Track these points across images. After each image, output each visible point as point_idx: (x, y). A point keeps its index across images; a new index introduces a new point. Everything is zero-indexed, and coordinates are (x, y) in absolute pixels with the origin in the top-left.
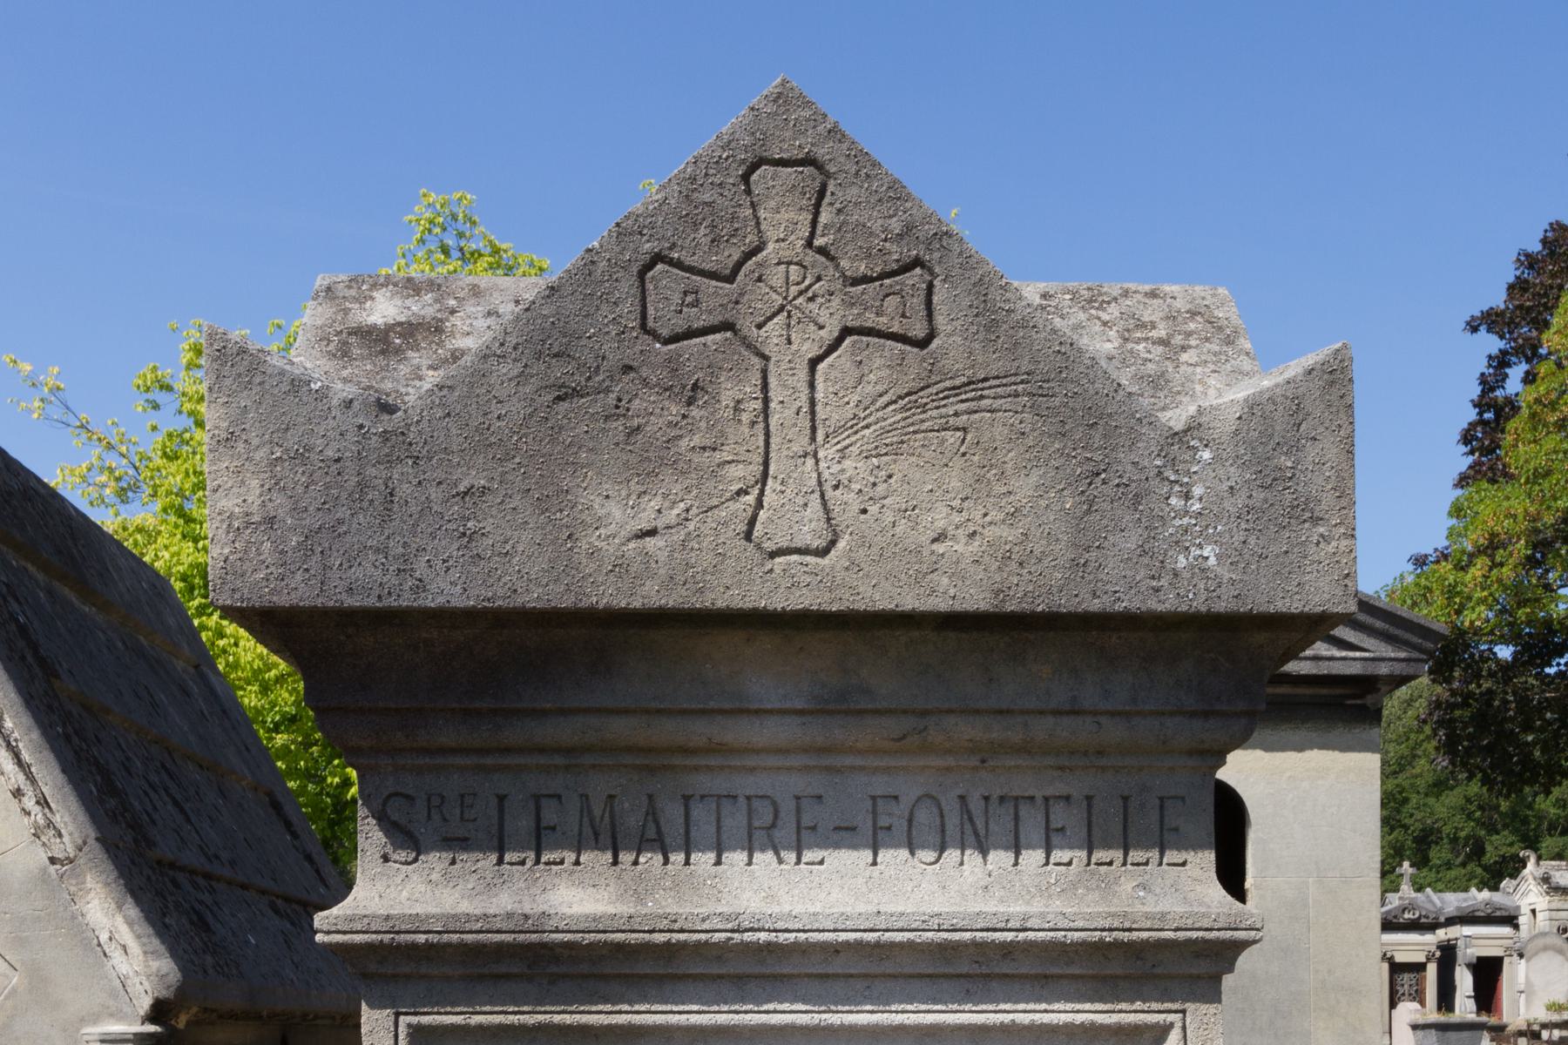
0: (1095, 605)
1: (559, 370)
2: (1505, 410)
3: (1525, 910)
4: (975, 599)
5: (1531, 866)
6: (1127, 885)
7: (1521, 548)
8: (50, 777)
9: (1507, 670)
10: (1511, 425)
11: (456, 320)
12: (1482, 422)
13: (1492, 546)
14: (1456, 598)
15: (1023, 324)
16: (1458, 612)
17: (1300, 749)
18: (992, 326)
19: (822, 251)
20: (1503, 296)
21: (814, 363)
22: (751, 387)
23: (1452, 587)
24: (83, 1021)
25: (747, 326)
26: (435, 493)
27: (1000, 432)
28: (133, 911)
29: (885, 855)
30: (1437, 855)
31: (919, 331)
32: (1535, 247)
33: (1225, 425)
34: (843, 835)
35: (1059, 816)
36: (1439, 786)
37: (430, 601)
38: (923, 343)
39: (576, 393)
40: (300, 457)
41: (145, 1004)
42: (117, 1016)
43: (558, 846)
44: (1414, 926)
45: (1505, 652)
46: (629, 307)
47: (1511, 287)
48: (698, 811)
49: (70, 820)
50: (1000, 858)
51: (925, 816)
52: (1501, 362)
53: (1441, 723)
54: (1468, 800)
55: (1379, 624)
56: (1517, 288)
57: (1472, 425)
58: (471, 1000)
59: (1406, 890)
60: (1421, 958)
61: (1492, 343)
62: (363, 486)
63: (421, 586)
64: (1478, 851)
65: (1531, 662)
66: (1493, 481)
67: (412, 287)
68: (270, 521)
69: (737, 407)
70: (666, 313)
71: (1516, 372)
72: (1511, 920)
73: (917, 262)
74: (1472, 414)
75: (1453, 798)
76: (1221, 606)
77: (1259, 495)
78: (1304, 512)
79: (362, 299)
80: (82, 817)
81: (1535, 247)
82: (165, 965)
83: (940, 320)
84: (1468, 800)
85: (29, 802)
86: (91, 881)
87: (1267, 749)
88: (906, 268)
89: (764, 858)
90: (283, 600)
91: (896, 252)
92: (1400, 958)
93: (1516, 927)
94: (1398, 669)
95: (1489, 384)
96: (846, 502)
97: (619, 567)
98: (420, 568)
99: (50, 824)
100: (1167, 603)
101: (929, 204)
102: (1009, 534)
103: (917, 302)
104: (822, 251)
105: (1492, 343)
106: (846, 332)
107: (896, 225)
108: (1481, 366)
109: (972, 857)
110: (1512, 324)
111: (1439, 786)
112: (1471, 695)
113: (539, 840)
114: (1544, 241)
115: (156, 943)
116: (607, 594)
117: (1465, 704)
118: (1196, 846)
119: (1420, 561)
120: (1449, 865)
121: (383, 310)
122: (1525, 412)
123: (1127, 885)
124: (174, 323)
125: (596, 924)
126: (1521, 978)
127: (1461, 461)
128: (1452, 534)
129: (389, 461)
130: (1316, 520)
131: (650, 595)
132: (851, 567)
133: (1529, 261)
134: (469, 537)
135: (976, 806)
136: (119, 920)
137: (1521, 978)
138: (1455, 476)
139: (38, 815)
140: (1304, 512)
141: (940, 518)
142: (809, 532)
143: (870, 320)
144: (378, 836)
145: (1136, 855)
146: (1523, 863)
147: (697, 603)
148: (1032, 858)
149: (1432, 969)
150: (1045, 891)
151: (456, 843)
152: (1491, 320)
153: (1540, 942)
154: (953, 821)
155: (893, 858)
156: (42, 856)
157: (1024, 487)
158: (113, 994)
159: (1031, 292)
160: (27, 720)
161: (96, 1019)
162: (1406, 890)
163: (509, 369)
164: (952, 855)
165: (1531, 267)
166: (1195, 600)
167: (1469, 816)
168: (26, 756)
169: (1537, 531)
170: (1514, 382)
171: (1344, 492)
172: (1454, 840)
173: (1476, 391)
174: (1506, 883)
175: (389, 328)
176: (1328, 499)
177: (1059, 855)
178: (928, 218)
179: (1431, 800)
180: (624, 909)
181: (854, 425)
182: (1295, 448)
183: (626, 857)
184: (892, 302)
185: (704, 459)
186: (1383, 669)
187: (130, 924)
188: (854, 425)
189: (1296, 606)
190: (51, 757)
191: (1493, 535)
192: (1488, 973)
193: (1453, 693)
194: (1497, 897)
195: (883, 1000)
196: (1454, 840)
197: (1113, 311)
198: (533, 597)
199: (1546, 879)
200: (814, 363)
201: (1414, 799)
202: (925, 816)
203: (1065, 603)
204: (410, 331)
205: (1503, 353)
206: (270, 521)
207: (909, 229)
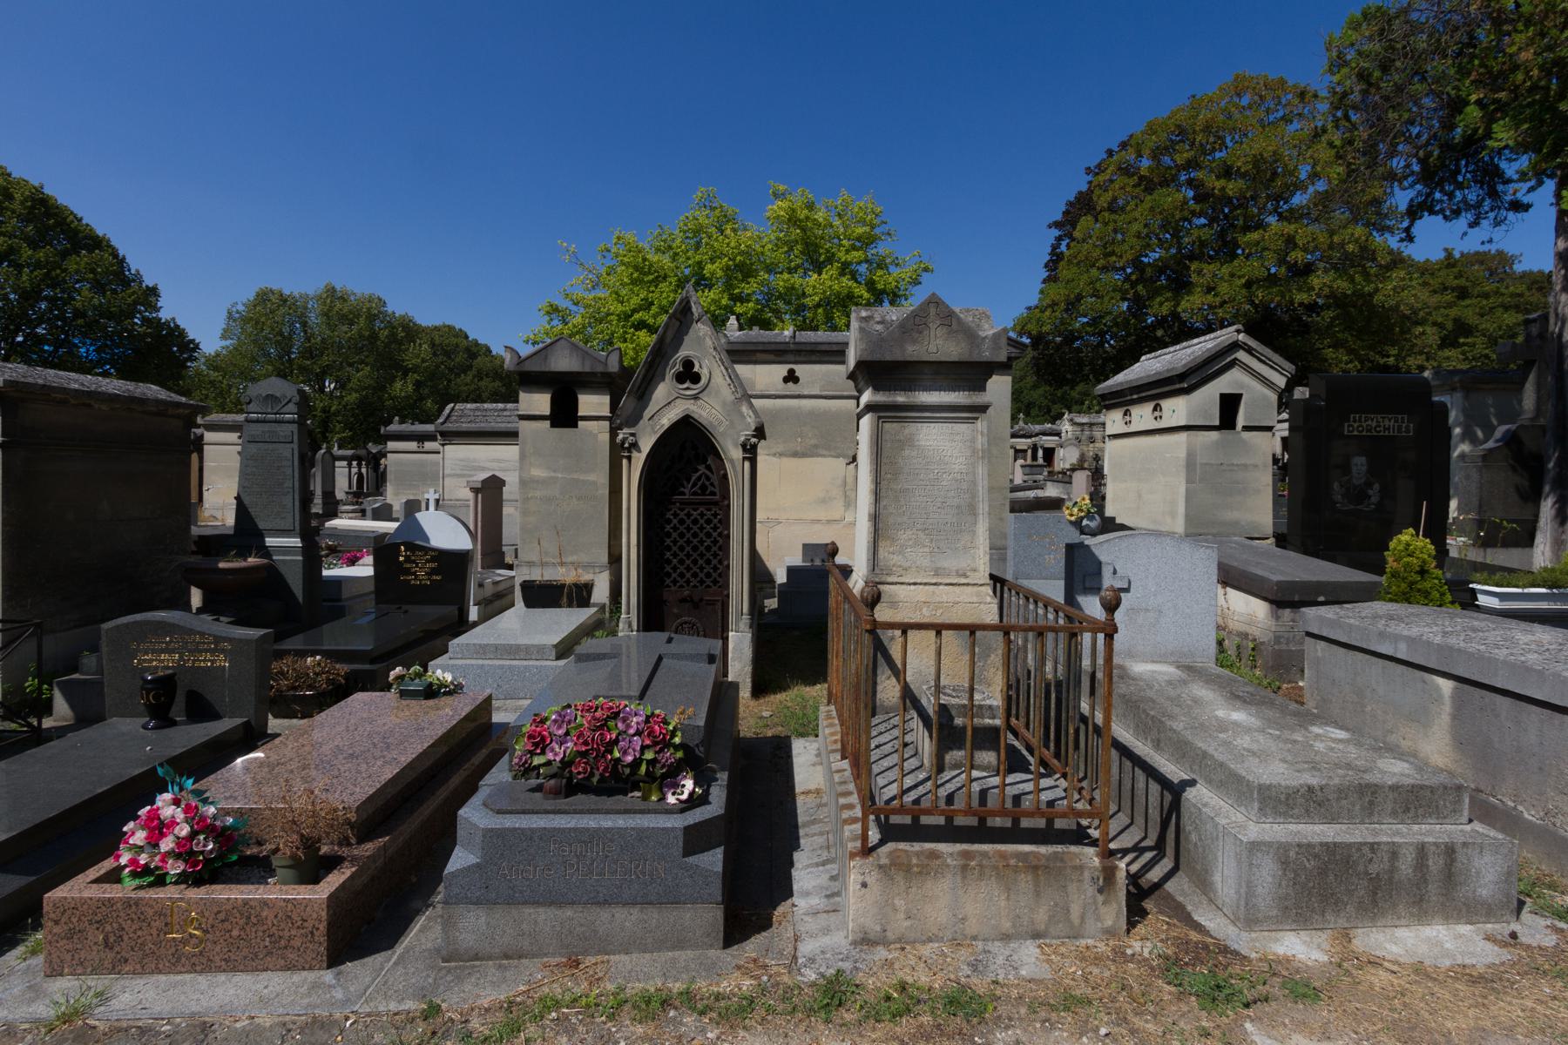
5: (1066, 416)
10: (1061, 263)
12: (1051, 260)
13: (1054, 304)
20: (1061, 215)
30: (1034, 412)
32: (1072, 199)
47: (1064, 213)
52: (1059, 239)
54: (1046, 392)
56: (1066, 213)
59: (1021, 423)
60: (1026, 448)
61: (1056, 233)
64: (1049, 411)
71: (1064, 244)
72: (1058, 434)
74: (1048, 258)
75: (1040, 391)
81: (1072, 199)
92: (1018, 448)
95: (1055, 247)
105: (1056, 233)
114: (1076, 198)
119: (1029, 308)
120: (1038, 416)
128: (1040, 299)
133: (1070, 204)
146: (1064, 414)
149: (1030, 452)
152: (1057, 225)
162: (1021, 423)
167: (1046, 398)
170: (1063, 248)
172: (1040, 407)
173: (1049, 249)
174: (1058, 422)
192: (1049, 454)
194: (1054, 427)
199: (1071, 420)
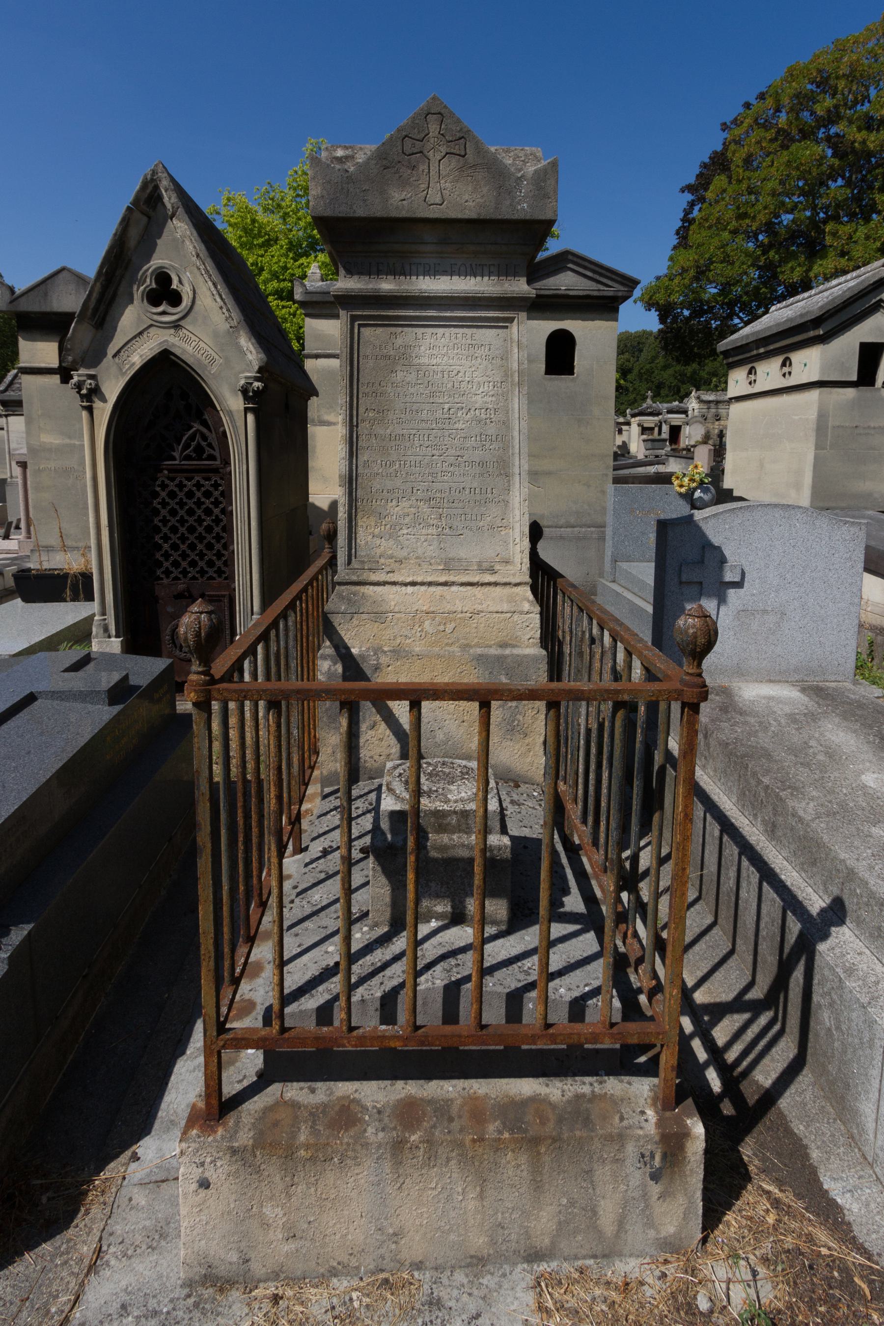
0: (500, 217)
1: (385, 162)
2: (691, 222)
3: (690, 409)
4: (473, 215)
5: (693, 393)
6: (506, 285)
7: (692, 273)
8: (231, 303)
9: (688, 319)
10: (692, 227)
11: (357, 155)
12: (683, 227)
14: (669, 291)
15: (486, 152)
16: (669, 296)
17: (593, 320)
18: (479, 152)
19: (442, 135)
20: (694, 179)
21: (440, 161)
22: (426, 167)
23: (667, 286)
24: (240, 373)
25: (425, 152)
26: (358, 191)
27: (480, 177)
28: (254, 341)
29: (454, 277)
30: (663, 392)
31: (463, 153)
32: (707, 160)
33: (530, 175)
34: (444, 273)
35: (492, 269)
36: (665, 367)
37: (357, 215)
38: (464, 156)
39: (388, 168)
40: (329, 182)
41: (257, 368)
42: (249, 371)
43: (382, 274)
44: (651, 414)
45: (686, 313)
46: (400, 147)
47: (697, 176)
48: (413, 267)
49: (236, 315)
50: (479, 278)
51: (462, 268)
52: (692, 204)
53: (662, 338)
54: (676, 372)
55: (619, 279)
56: (700, 176)
57: (680, 228)
58: (364, 309)
59: (649, 401)
60: (653, 425)
61: (689, 197)
62: (342, 189)
63: (355, 212)
64: (679, 391)
65: (696, 317)
66: (685, 248)
67: (346, 148)
68: (323, 196)
69: (423, 171)
70: (408, 149)
71: (697, 208)
72: (685, 412)
73: (463, 137)
74: (680, 224)
75: (670, 371)
76: (528, 218)
77: (537, 192)
78: (546, 196)
79: (335, 151)
80: (240, 314)
81: (707, 160)
82: (262, 356)
83: (468, 151)
84: (676, 372)
85: (224, 310)
86: (242, 333)
87: (583, 320)
88: (460, 138)
89: (427, 278)
90: (325, 215)
91: (458, 135)
92: (646, 425)
93: (687, 416)
94: (625, 294)
95: (687, 212)
96: (446, 193)
97: (397, 208)
98: (354, 207)
99: (230, 316)
100: (516, 217)
101: (466, 124)
102: (482, 201)
103: (462, 147)
104: (442, 135)
105: (689, 197)
106: (447, 153)
107: (458, 128)
108: (685, 205)
109: (473, 278)
110: (697, 190)
111: (665, 367)
112: (674, 328)
113: (379, 273)
114: (710, 158)
115: (260, 350)
116: (394, 214)
117: (671, 332)
118: (522, 276)
119: (658, 278)
120: (667, 396)
121: (340, 153)
122: (697, 222)
123: (506, 285)
124: (220, 189)
125: (390, 291)
126: (687, 432)
127: (675, 241)
128: (669, 268)
129: (348, 183)
130: (549, 198)
131: (404, 214)
132: (448, 208)
133: (704, 166)
134: (365, 201)
135: (474, 266)
136: (250, 344)
137: (687, 432)
138: (672, 246)
139: (227, 314)
140: (546, 196)
141: (466, 197)
142: (438, 200)
143: (452, 151)
144: (344, 272)
145: (509, 278)
146: (691, 393)
147: (414, 216)
148: (486, 278)
149: (656, 429)
150: (488, 286)
151: (360, 273)
152: (689, 188)
153: (694, 420)
154: (468, 270)
155: (455, 278)
156: (228, 326)
157: (485, 190)
158: (248, 365)
159: (493, 149)
160: (224, 286)
161: (243, 372)
162: (649, 401)
163: (374, 162)
164: (468, 278)
165: (705, 168)
166: (521, 216)
167: (676, 378)
168: (224, 297)
169: (698, 267)
170: (696, 213)
171: (555, 191)
172: (670, 387)
173: (682, 215)
174: (685, 400)
175: (342, 157)
176: (552, 193)
177: (492, 278)
178: (465, 127)
179: (662, 372)
180: (397, 288)
181: (448, 175)
182: (545, 181)
183: (397, 277)
184: (457, 147)
185: (416, 183)
186: (620, 294)
187: (253, 344)
188: (448, 175)
189: (543, 218)
190: (231, 296)
191: (683, 268)
192: (675, 431)
193: (667, 327)
194: (682, 405)
195: (452, 310)
196: (670, 387)
197: (512, 153)
198: (378, 214)
199: (698, 398)
200: (440, 161)
201: (656, 372)
202: (462, 268)
203: (493, 217)
204: (347, 158)
205: (693, 201)
206: (323, 196)
207: (461, 129)
